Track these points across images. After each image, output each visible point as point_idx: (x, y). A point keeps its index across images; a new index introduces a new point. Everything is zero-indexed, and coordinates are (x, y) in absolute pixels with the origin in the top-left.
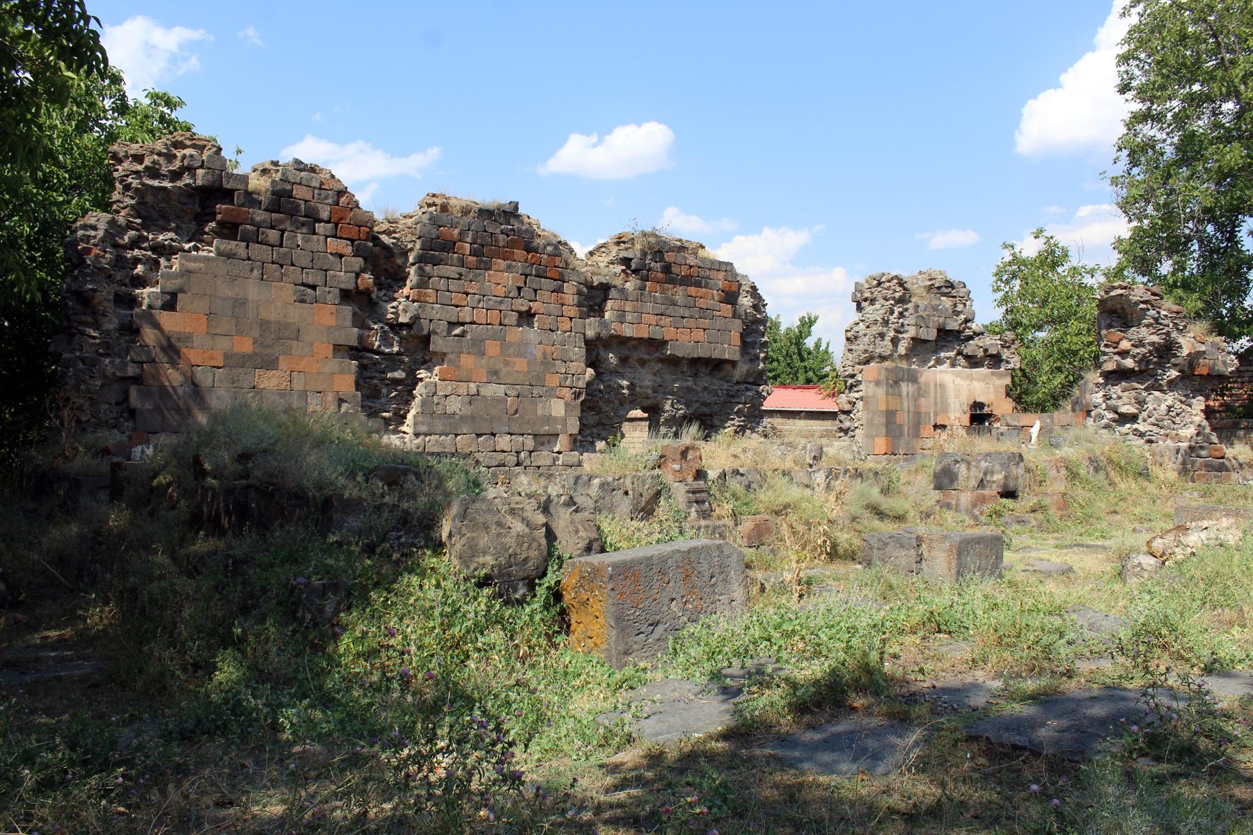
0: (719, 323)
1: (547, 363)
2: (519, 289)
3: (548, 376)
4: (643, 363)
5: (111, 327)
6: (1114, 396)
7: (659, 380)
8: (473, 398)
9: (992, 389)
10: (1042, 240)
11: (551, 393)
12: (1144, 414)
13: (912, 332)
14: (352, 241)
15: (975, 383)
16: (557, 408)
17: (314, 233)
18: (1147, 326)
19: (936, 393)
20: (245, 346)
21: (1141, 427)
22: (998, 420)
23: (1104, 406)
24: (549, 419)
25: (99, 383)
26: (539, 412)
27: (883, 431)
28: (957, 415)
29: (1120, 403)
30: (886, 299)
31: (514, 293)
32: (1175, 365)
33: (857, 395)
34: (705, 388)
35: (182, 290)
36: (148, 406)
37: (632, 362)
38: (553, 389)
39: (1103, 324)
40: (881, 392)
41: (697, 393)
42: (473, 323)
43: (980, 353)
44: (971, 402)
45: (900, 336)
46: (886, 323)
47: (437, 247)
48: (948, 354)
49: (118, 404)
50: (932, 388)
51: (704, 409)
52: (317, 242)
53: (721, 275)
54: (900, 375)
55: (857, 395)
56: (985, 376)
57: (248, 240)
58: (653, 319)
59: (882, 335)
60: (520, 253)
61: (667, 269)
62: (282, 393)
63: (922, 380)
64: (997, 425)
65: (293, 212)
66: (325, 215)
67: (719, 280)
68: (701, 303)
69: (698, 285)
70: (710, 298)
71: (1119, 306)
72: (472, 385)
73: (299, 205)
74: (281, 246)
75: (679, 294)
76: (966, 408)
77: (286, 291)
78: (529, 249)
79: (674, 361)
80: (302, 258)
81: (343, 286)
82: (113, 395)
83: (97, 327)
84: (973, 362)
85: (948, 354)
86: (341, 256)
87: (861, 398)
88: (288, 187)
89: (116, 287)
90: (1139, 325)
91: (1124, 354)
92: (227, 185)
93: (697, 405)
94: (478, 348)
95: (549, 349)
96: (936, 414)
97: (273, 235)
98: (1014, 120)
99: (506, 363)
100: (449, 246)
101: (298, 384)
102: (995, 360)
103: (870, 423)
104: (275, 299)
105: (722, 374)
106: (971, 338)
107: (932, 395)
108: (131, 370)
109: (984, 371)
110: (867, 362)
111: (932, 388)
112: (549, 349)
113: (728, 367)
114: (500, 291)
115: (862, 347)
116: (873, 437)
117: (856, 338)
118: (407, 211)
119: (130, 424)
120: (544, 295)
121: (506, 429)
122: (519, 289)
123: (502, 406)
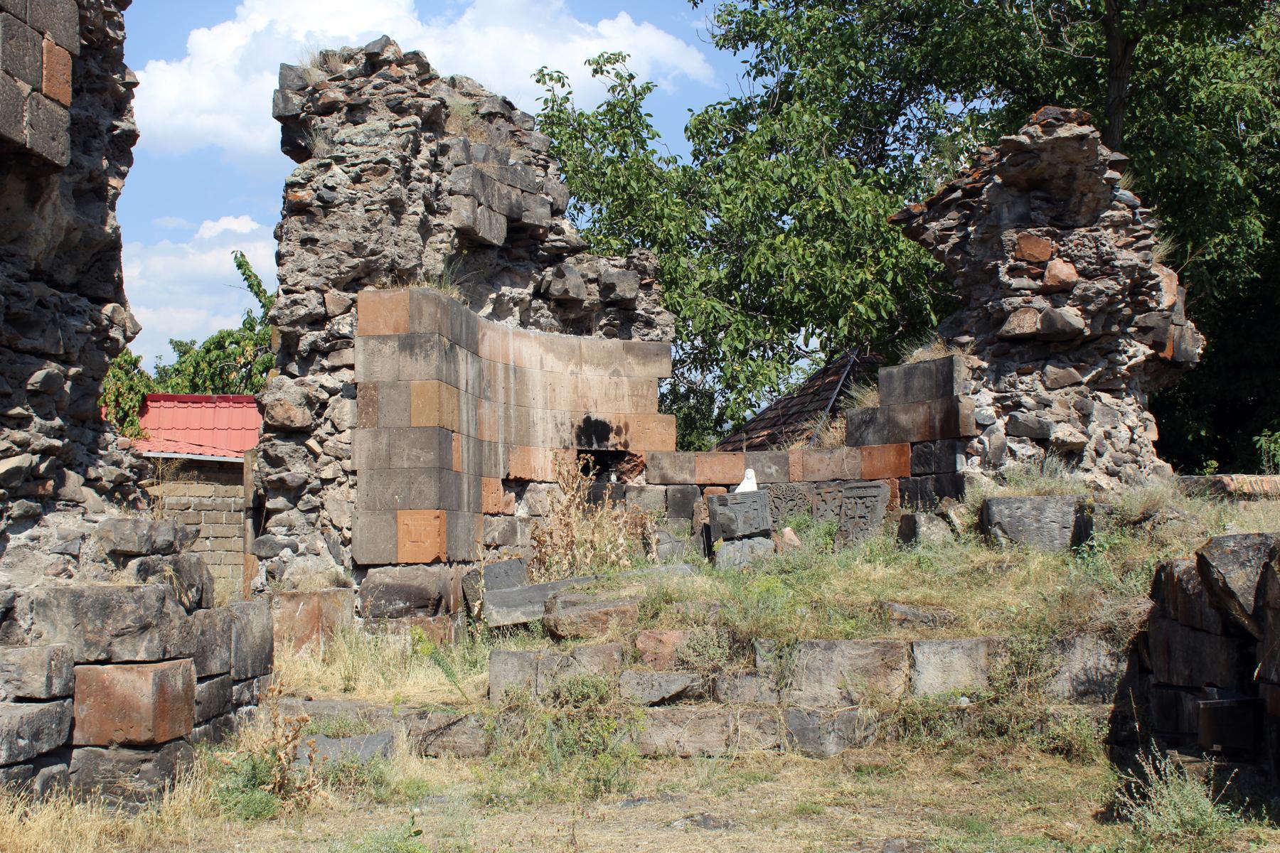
9: (626, 389)
10: (609, 80)
15: (589, 372)
18: (1116, 226)
19: (507, 389)
23: (1001, 423)
27: (430, 489)
28: (548, 458)
30: (399, 109)
32: (1144, 330)
39: (1006, 215)
43: (591, 295)
44: (579, 421)
45: (435, 220)
46: (405, 175)
48: (517, 292)
50: (501, 373)
56: (610, 353)
59: (396, 207)
64: (636, 481)
71: (1063, 169)
76: (569, 435)
84: (573, 317)
85: (517, 292)
87: (350, 391)
90: (1093, 220)
102: (621, 317)
103: (383, 467)
107: (501, 396)
109: (595, 342)
110: (353, 283)
111: (501, 373)
115: (343, 236)
116: (391, 510)
117: (327, 205)
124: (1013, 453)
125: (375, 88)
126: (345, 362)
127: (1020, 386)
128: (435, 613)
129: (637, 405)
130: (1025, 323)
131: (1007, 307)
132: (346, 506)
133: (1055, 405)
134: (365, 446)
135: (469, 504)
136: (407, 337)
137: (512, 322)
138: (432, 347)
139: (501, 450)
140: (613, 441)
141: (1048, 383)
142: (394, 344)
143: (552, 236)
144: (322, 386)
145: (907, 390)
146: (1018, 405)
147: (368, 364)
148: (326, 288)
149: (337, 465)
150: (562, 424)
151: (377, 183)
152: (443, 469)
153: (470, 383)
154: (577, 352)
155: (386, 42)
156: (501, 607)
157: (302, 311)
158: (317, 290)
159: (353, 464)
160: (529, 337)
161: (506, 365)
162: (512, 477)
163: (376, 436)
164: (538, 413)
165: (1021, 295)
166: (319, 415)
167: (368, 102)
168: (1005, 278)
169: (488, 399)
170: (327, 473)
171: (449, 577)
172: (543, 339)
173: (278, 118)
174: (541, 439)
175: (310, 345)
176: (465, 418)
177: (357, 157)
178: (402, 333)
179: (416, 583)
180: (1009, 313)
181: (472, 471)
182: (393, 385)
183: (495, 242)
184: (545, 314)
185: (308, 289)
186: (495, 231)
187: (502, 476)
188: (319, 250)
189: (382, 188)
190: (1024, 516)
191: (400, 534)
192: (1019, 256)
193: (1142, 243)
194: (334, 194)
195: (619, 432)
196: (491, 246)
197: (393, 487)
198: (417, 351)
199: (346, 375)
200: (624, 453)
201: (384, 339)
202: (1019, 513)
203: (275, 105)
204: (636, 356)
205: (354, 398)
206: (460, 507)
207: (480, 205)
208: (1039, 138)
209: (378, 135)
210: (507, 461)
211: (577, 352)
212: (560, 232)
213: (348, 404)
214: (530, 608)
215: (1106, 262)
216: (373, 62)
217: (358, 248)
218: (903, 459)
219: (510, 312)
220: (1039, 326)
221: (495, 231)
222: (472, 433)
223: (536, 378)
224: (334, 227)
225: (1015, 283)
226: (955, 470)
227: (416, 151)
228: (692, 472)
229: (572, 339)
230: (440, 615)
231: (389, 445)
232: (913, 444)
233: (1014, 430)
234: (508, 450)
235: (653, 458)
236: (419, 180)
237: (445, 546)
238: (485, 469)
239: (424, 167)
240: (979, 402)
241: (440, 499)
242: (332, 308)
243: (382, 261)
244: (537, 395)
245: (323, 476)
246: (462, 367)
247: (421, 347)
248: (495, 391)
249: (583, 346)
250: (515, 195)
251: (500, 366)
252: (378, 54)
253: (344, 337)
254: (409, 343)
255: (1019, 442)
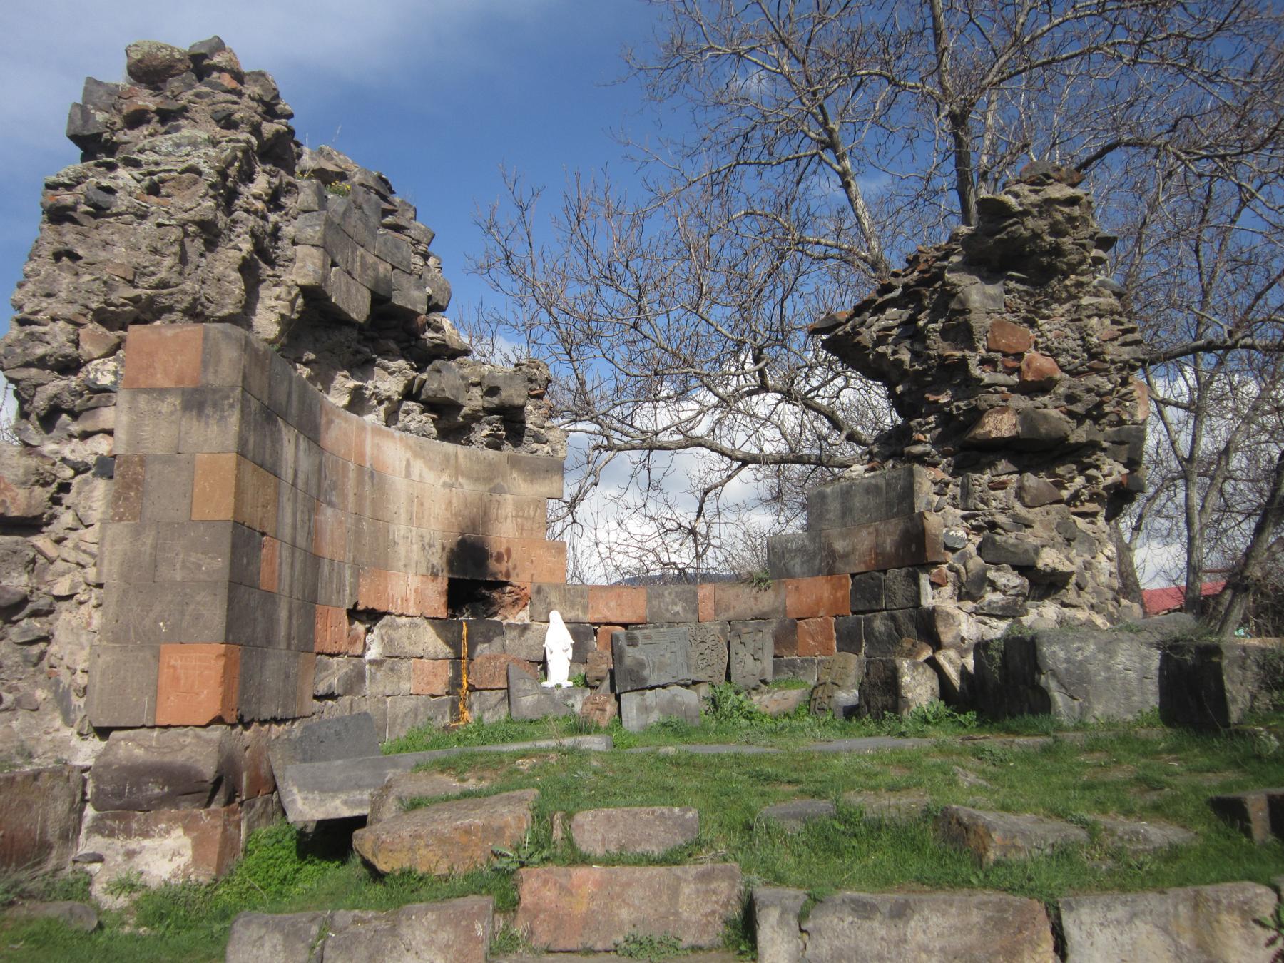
13: (304, 266)
27: (215, 613)
40: (216, 438)
44: (450, 542)
76: (438, 559)
84: (450, 422)
87: (105, 467)
103: (143, 579)
124: (994, 586)
125: (198, 95)
126: (101, 426)
127: (994, 503)
128: (208, 804)
129: (522, 528)
130: (1000, 425)
131: (984, 405)
132: (84, 638)
133: (1037, 526)
134: (119, 547)
135: (289, 638)
136: (195, 391)
137: (373, 419)
138: (232, 406)
139: (348, 573)
141: (1027, 499)
142: (174, 401)
143: (430, 334)
144: (64, 460)
145: (846, 511)
146: (993, 526)
147: (134, 429)
148: (82, 320)
149: (78, 576)
150: (430, 546)
152: (241, 584)
153: (301, 476)
154: (453, 462)
155: (219, 46)
156: (312, 791)
157: (40, 350)
158: (69, 321)
159: (99, 573)
160: (393, 436)
162: (360, 607)
163: (137, 533)
164: (400, 529)
165: (996, 392)
166: (56, 501)
167: (185, 109)
168: (976, 372)
169: (330, 504)
170: (62, 588)
171: (240, 746)
172: (411, 442)
173: (76, 138)
174: (402, 563)
175: (51, 399)
176: (288, 519)
177: (157, 164)
178: (188, 385)
179: (180, 758)
180: (985, 411)
181: (296, 594)
182: (166, 461)
183: (354, 315)
184: (416, 416)
185: (54, 319)
186: (358, 306)
187: (348, 605)
188: (81, 270)
189: (188, 205)
190: (1086, 659)
191: (164, 679)
192: (993, 346)
193: (1130, 337)
194: (111, 198)
195: (499, 558)
196: (351, 323)
197: (157, 608)
198: (209, 411)
199: (102, 446)
200: (506, 584)
201: (162, 392)
202: (1080, 657)
203: (71, 121)
204: (522, 471)
205: (111, 477)
206: (269, 640)
207: (334, 264)
208: (1026, 197)
209: (195, 145)
210: (355, 587)
211: (453, 462)
212: (439, 329)
213: (100, 489)
214: (357, 795)
215: (1093, 356)
216: (199, 64)
218: (839, 594)
219: (371, 410)
220: (1019, 429)
221: (358, 306)
222: (301, 541)
223: (399, 485)
224: (106, 244)
225: (987, 376)
226: (917, 605)
227: (248, 177)
228: (585, 608)
229: (449, 447)
230: (213, 807)
231: (155, 547)
232: (853, 575)
234: (357, 574)
235: (539, 591)
236: (247, 211)
237: (235, 697)
238: (322, 594)
239: (256, 197)
240: (947, 523)
241: (229, 629)
242: (87, 348)
243: (178, 297)
244: (399, 504)
245: (55, 592)
246: (288, 451)
247: (215, 405)
248: (344, 497)
249: (460, 454)
250: (383, 268)
251: (352, 466)
252: (204, 56)
253: (105, 390)
254: (197, 401)
255: (998, 570)
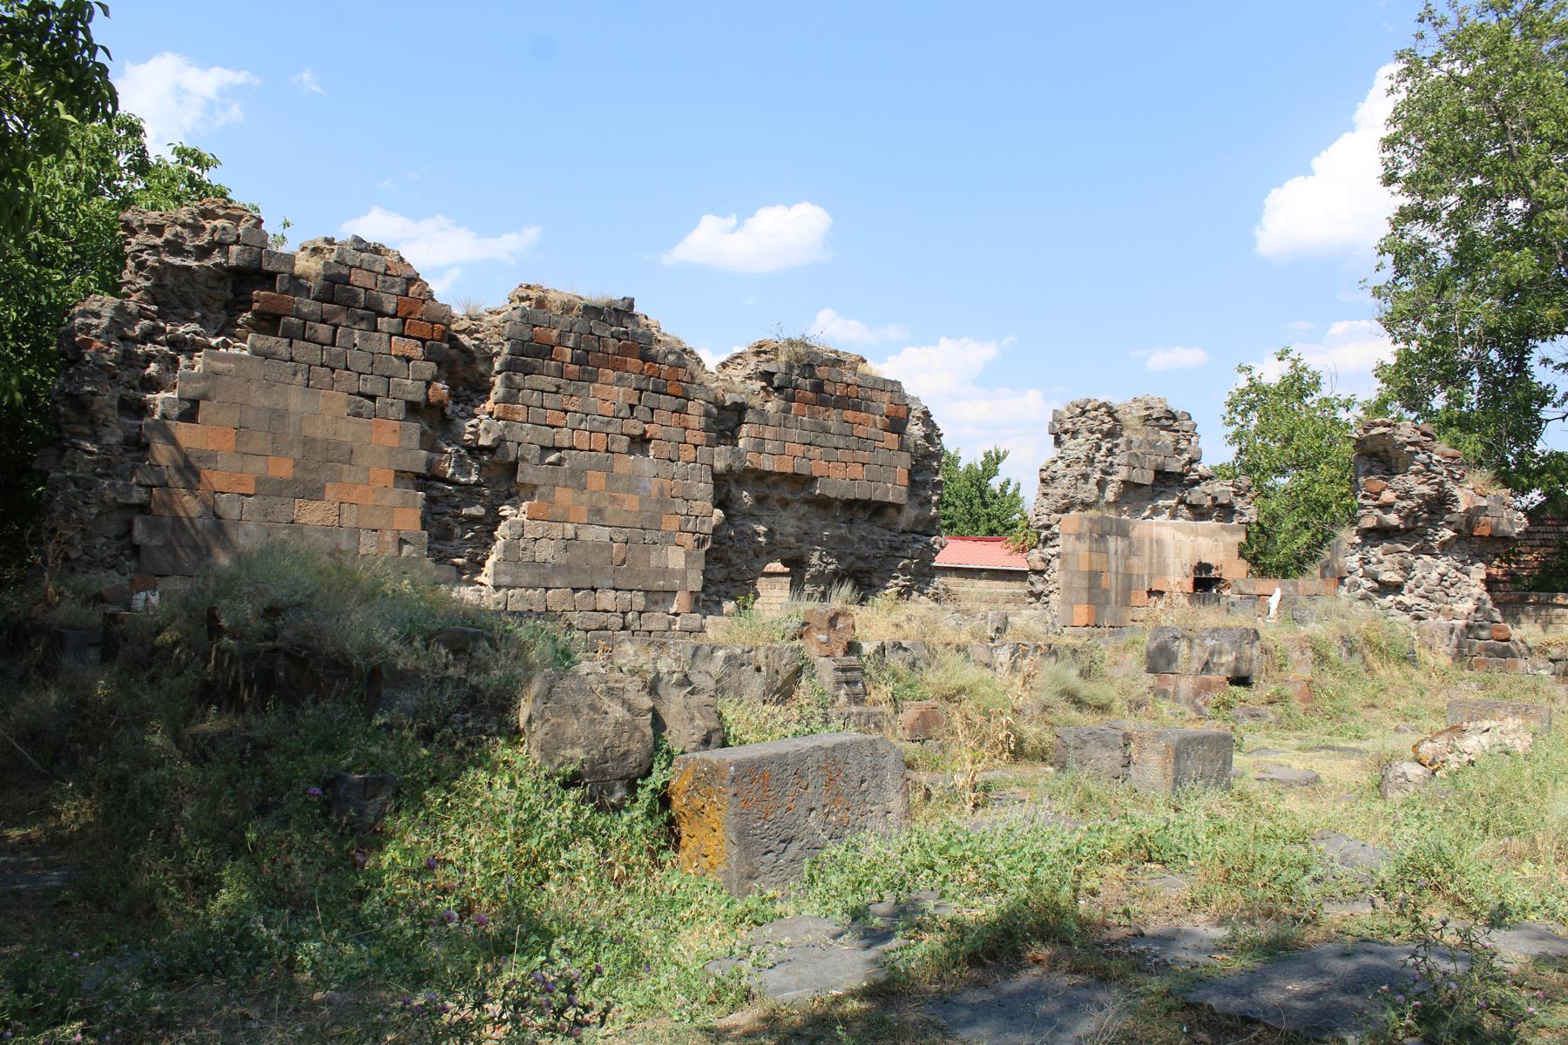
0: (882, 457)
1: (664, 501)
2: (632, 407)
3: (665, 517)
4: (785, 504)
5: (113, 440)
6: (1374, 560)
7: (804, 526)
8: (569, 543)
10: (1287, 363)
11: (668, 539)
12: (1411, 583)
13: (1123, 473)
14: (423, 341)
15: (1201, 540)
16: (676, 558)
17: (376, 330)
18: (1416, 473)
19: (1151, 550)
20: (283, 469)
21: (1407, 599)
22: (1228, 586)
24: (665, 572)
25: (95, 510)
26: (653, 563)
27: (1085, 595)
28: (1178, 579)
29: (1381, 568)
30: (1091, 432)
31: (625, 412)
32: (1450, 523)
33: (1052, 551)
34: (863, 538)
35: (205, 397)
36: (156, 542)
37: (772, 502)
38: (670, 533)
39: (1361, 470)
40: (1083, 547)
41: (852, 543)
42: (572, 448)
43: (1208, 502)
46: (1090, 461)
47: (530, 352)
48: (1168, 503)
49: (118, 538)
51: (861, 564)
52: (378, 342)
53: (886, 397)
54: (1107, 528)
55: (1052, 551)
57: (291, 335)
58: (798, 449)
59: (1086, 477)
60: (633, 362)
61: (818, 387)
62: (327, 530)
63: (1134, 533)
64: (1226, 592)
65: (349, 303)
66: (390, 307)
67: (884, 402)
68: (860, 431)
69: (856, 408)
70: (871, 425)
71: (1380, 448)
72: (569, 526)
73: (355, 298)
74: (333, 344)
75: (833, 418)
76: (1189, 570)
77: (338, 401)
78: (646, 358)
79: (824, 503)
80: (359, 360)
81: (410, 398)
82: (113, 526)
83: (95, 439)
84: (1198, 513)
85: (1168, 503)
86: (409, 360)
87: (1058, 555)
88: (345, 271)
89: (121, 390)
90: (1405, 472)
91: (1386, 507)
92: (267, 267)
93: (852, 558)
94: (577, 480)
95: (667, 484)
96: (1151, 577)
97: (324, 331)
98: (1254, 213)
99: (613, 500)
100: (545, 351)
101: (349, 519)
102: (1226, 511)
103: (1069, 586)
104: (323, 412)
105: (884, 521)
106: (1196, 483)
107: (1147, 553)
108: (138, 496)
109: (1212, 524)
110: (1066, 510)
112: (667, 484)
113: (891, 511)
114: (608, 409)
115: (1060, 491)
116: (1071, 604)
117: (1053, 479)
118: (493, 307)
119: (133, 564)
120: (663, 416)
121: (610, 583)
122: (632, 407)
123: (606, 554)
140: (1214, 573)
151: (1076, 467)
161: (1151, 540)
217: (1065, 496)
233: (1366, 575)
250: (1160, 460)
